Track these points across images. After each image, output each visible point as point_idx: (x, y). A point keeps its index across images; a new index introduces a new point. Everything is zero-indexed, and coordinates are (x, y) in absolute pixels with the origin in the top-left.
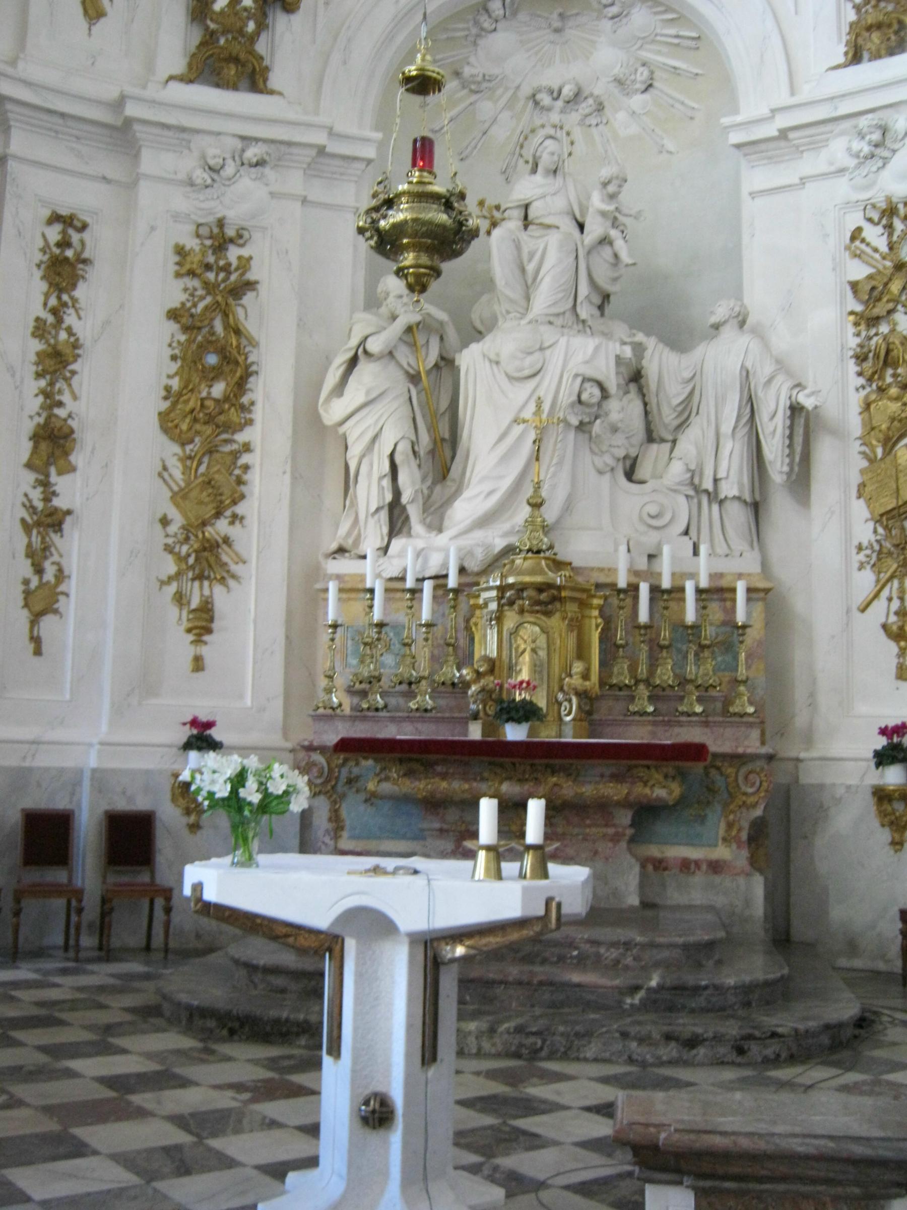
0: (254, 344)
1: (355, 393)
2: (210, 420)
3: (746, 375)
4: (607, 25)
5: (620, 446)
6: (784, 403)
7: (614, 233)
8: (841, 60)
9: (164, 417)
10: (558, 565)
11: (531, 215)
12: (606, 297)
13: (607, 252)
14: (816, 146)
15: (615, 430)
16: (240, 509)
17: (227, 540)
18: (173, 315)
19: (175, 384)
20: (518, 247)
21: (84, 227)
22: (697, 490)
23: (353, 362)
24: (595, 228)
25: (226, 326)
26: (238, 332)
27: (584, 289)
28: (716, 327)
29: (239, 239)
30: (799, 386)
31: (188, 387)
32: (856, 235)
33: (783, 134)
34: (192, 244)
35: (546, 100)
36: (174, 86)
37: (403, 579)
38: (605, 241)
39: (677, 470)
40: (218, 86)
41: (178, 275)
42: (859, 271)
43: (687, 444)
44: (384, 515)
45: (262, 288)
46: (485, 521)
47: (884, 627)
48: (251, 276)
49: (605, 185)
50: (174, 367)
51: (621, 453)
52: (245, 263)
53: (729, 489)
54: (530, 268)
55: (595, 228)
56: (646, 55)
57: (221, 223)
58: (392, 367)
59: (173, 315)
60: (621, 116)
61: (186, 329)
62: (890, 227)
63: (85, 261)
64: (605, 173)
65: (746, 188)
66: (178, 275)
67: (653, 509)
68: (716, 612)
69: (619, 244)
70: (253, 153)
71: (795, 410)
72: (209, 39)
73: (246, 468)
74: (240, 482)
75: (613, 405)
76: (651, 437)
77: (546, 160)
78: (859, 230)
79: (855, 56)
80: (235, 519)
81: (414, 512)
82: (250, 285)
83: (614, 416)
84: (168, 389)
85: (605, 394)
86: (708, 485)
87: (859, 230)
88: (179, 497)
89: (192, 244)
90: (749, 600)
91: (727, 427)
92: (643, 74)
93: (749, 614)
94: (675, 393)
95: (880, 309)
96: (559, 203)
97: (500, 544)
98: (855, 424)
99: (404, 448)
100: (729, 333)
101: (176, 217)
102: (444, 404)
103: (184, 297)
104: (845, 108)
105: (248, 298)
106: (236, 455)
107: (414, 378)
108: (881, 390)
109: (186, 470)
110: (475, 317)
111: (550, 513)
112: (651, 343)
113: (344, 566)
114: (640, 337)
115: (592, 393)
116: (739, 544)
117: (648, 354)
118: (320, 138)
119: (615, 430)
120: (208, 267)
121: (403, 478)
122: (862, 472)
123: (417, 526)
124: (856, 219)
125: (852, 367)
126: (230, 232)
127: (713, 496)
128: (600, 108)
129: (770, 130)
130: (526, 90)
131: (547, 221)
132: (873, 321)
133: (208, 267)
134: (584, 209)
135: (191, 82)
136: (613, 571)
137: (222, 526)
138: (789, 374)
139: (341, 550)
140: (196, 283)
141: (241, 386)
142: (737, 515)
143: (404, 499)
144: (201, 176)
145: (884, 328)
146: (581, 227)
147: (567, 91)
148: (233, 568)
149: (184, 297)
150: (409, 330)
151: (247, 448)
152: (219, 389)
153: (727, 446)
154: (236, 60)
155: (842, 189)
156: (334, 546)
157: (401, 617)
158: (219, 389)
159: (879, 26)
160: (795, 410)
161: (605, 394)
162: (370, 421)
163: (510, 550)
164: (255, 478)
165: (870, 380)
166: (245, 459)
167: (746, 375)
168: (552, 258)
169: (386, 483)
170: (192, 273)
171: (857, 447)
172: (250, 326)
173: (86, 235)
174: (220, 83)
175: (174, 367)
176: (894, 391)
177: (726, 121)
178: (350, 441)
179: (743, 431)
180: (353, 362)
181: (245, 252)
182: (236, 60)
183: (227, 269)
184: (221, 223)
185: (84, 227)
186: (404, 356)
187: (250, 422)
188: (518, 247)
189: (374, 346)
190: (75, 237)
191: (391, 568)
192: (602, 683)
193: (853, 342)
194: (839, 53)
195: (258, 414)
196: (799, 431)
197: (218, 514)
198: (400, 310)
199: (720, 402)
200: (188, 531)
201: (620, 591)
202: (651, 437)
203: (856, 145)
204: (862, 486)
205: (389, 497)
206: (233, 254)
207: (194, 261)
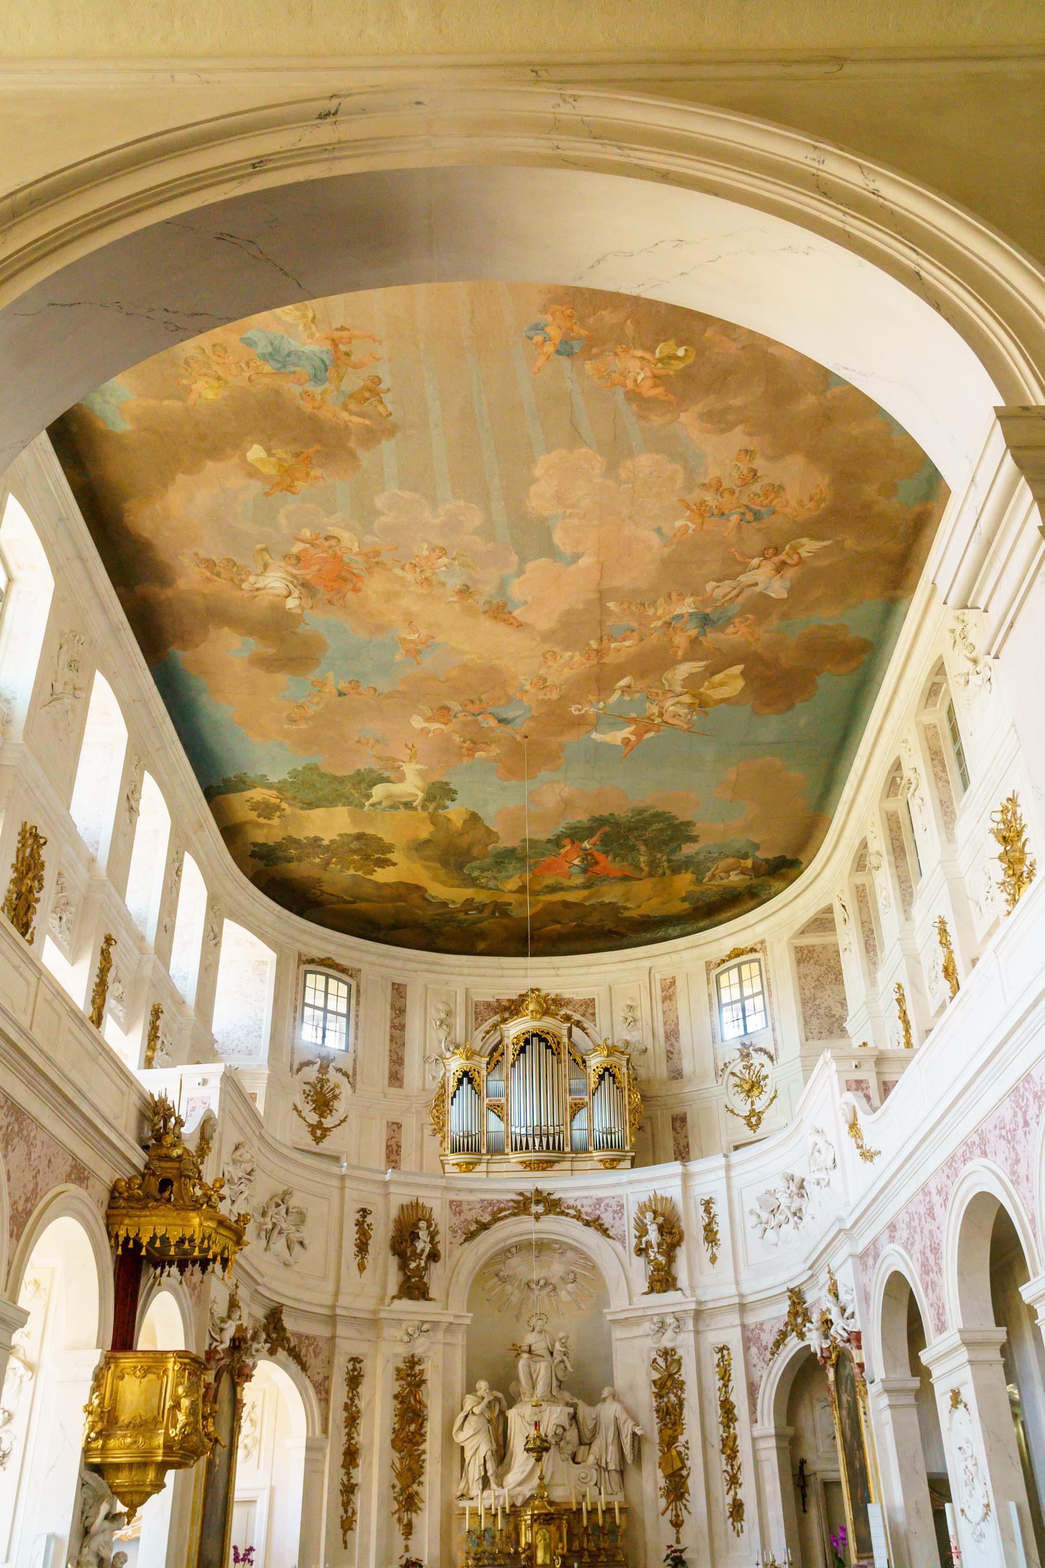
0: (426, 1407)
1: (468, 1431)
2: (410, 1441)
3: (616, 1419)
4: (557, 1256)
5: (569, 1449)
6: (630, 1432)
7: (565, 1358)
8: (646, 1290)
9: (393, 1441)
10: (551, 1503)
11: (533, 1348)
12: (561, 1382)
13: (562, 1366)
14: (639, 1324)
15: (568, 1443)
16: (421, 1479)
17: (417, 1493)
18: (396, 1397)
19: (397, 1426)
20: (529, 1366)
21: (361, 1361)
22: (600, 1466)
23: (466, 1416)
24: (558, 1357)
25: (415, 1399)
26: (420, 1402)
27: (555, 1383)
28: (604, 1400)
29: (419, 1362)
30: (637, 1424)
31: (402, 1428)
32: (654, 1361)
33: (627, 1318)
34: (402, 1366)
35: (533, 1286)
36: (396, 1301)
37: (490, 1509)
38: (562, 1361)
39: (591, 1459)
40: (411, 1298)
41: (397, 1380)
42: (656, 1376)
43: (595, 1447)
44: (480, 1481)
45: (429, 1383)
46: (521, 1484)
47: (671, 1521)
48: (424, 1378)
49: (561, 1339)
50: (396, 1419)
51: (570, 1452)
52: (422, 1372)
53: (612, 1466)
54: (534, 1376)
55: (558, 1357)
56: (573, 1268)
57: (413, 1356)
58: (482, 1418)
59: (396, 1397)
60: (563, 1292)
61: (401, 1403)
62: (666, 1360)
63: (362, 1376)
64: (561, 1335)
65: (613, 1338)
66: (397, 1380)
67: (583, 1475)
68: (609, 1519)
69: (567, 1363)
70: (425, 1327)
71: (634, 1434)
72: (408, 1278)
73: (424, 1461)
74: (421, 1467)
75: (567, 1434)
76: (581, 1443)
77: (537, 1329)
78: (655, 1359)
79: (652, 1290)
80: (420, 1483)
81: (492, 1480)
82: (424, 1382)
83: (568, 1439)
84: (394, 1429)
85: (565, 1430)
86: (603, 1465)
87: (655, 1359)
88: (399, 1475)
89: (402, 1366)
90: (620, 1513)
91: (610, 1441)
92: (571, 1276)
93: (620, 1519)
94: (590, 1425)
95: (664, 1392)
96: (544, 1345)
97: (528, 1495)
98: (656, 1438)
99: (489, 1453)
100: (609, 1401)
101: (396, 1355)
102: (501, 1429)
103: (399, 1389)
104: (649, 1312)
105: (423, 1387)
106: (420, 1455)
107: (489, 1421)
108: (665, 1425)
109: (401, 1463)
110: (511, 1391)
111: (546, 1481)
112: (580, 1403)
113: (465, 1504)
114: (576, 1400)
115: (560, 1431)
116: (616, 1488)
117: (579, 1407)
118: (451, 1319)
119: (568, 1443)
120: (408, 1375)
121: (489, 1465)
122: (660, 1458)
123: (493, 1485)
124: (654, 1355)
125: (655, 1415)
126: (416, 1360)
127: (606, 1469)
128: (555, 1289)
129: (624, 1315)
130: (525, 1281)
131: (538, 1352)
132: (661, 1397)
133: (408, 1375)
134: (553, 1346)
135: (400, 1298)
136: (570, 1503)
137: (415, 1487)
138: (634, 1420)
139: (462, 1495)
140: (403, 1382)
141: (421, 1426)
142: (615, 1476)
143: (489, 1474)
144: (406, 1338)
145: (666, 1400)
146: (552, 1354)
147: (542, 1282)
148: (420, 1505)
149: (399, 1389)
150: (490, 1402)
151: (424, 1452)
152: (413, 1427)
153: (610, 1448)
154: (418, 1289)
155: (649, 1342)
156: (459, 1493)
157: (490, 1525)
158: (413, 1427)
159: (659, 1281)
160: (634, 1434)
161: (565, 1430)
162: (475, 1441)
163: (532, 1497)
164: (427, 1466)
165: (661, 1420)
166: (423, 1457)
167: (616, 1419)
168: (543, 1372)
169: (482, 1468)
170: (402, 1379)
171: (658, 1447)
172: (424, 1399)
173: (361, 1365)
174: (411, 1298)
175: (396, 1419)
176: (670, 1426)
177: (605, 1311)
178: (466, 1450)
179: (616, 1442)
180: (466, 1416)
181: (421, 1367)
182: (418, 1289)
183: (415, 1376)
184: (413, 1356)
185: (361, 1361)
186: (487, 1415)
187: (425, 1441)
188: (529, 1366)
189: (476, 1410)
190: (358, 1366)
191: (487, 1504)
192: (569, 1550)
193: (655, 1404)
194: (645, 1287)
195: (428, 1437)
196: (636, 1443)
197: (414, 1482)
198: (486, 1396)
199: (607, 1429)
200: (403, 1490)
201: (574, 1513)
202: (581, 1443)
203: (653, 1327)
204: (660, 1464)
205: (483, 1473)
206: (417, 1368)
207: (403, 1374)
